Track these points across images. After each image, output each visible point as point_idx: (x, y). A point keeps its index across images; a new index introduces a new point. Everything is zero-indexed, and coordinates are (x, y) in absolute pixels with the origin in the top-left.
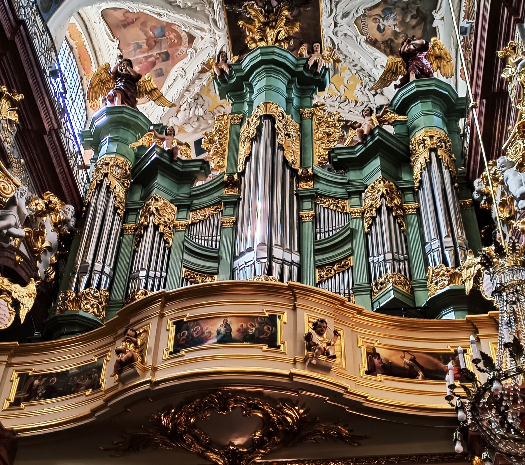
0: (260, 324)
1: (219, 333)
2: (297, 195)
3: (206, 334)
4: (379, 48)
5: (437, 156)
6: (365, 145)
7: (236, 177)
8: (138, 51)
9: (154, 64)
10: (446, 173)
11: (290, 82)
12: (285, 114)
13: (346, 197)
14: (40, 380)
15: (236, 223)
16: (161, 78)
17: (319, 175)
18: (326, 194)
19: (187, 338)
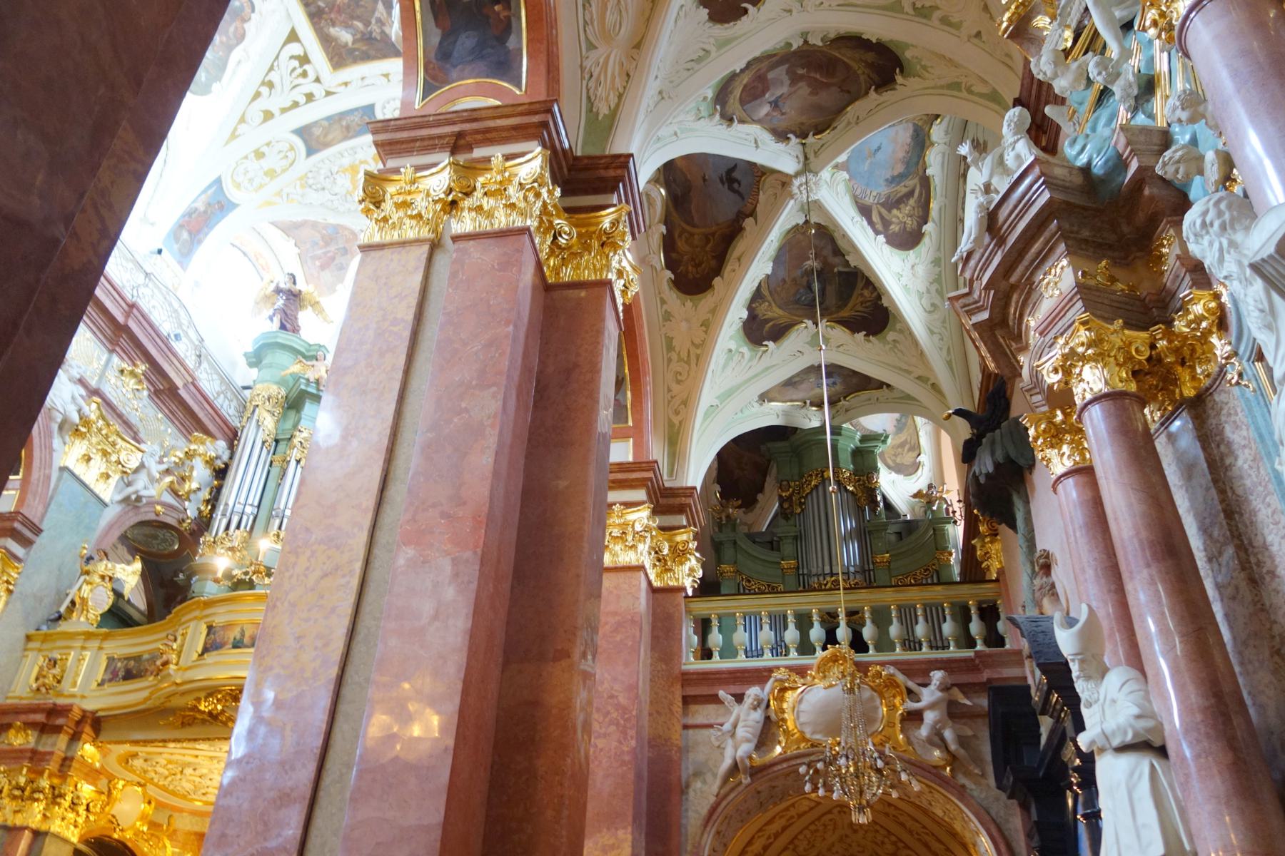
9: (333, 259)
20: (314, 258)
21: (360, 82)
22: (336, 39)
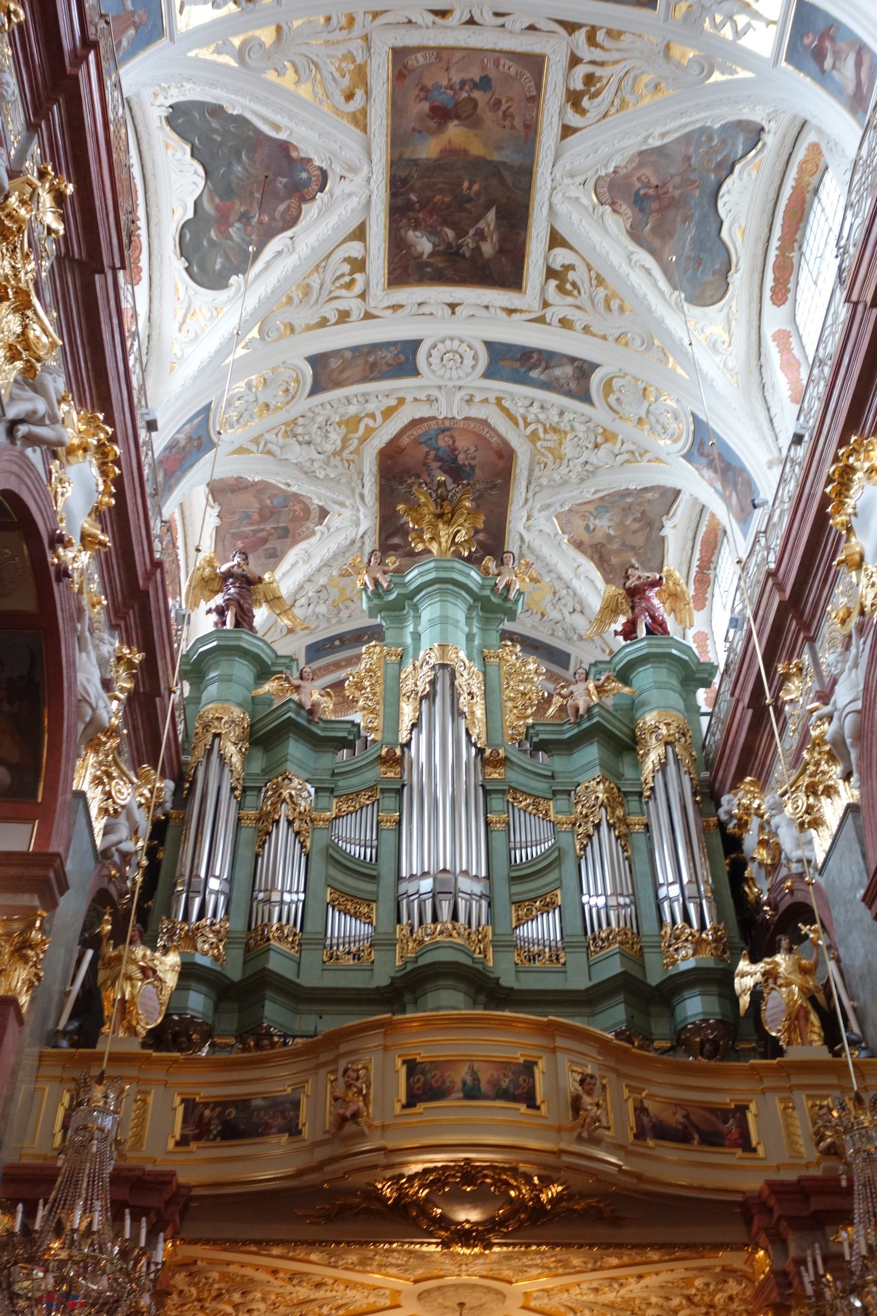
0: (514, 1073)
1: (464, 1083)
2: (483, 786)
3: (448, 1084)
4: (584, 552)
5: (675, 755)
6: (578, 724)
7: (398, 751)
8: (245, 522)
9: (265, 541)
10: (686, 779)
11: (470, 608)
12: (467, 662)
13: (550, 796)
14: (213, 1110)
15: (399, 823)
16: (272, 560)
17: (513, 759)
18: (523, 789)
19: (425, 1086)
20: (236, 536)
21: (415, 310)
22: (410, 246)
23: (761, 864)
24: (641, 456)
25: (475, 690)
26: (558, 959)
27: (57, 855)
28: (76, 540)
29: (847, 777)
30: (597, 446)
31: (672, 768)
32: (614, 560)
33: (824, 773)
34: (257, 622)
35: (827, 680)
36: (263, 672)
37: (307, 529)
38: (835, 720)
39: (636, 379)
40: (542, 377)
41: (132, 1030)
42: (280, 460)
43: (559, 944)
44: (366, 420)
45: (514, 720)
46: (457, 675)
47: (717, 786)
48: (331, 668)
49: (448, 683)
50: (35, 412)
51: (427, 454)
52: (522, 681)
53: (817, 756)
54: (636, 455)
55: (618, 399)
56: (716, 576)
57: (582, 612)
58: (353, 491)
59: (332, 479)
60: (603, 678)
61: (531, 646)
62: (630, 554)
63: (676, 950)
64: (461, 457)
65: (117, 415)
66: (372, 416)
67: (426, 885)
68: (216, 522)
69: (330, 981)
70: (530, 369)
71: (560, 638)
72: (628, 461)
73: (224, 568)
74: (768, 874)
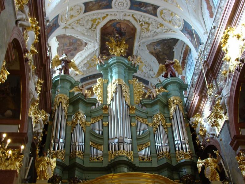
2: (129, 115)
5: (178, 108)
6: (154, 100)
8: (65, 46)
9: (70, 51)
13: (147, 118)
15: (108, 125)
16: (72, 56)
17: (137, 108)
18: (140, 116)
23: (201, 135)
24: (170, 30)
25: (127, 91)
26: (150, 159)
27: (26, 133)
28: (30, 51)
29: (225, 113)
30: (158, 28)
31: (178, 111)
32: (161, 57)
33: (219, 112)
34: (70, 72)
35: (220, 89)
36: (72, 86)
37: (82, 48)
38: (222, 99)
39: (169, 11)
40: (144, 9)
41: (45, 179)
42: (76, 30)
43: (150, 155)
44: (98, 20)
45: (138, 98)
46: (122, 86)
47: (189, 115)
48: (87, 84)
49: (120, 88)
50: (23, 18)
51: (114, 29)
52: (138, 88)
53: (217, 108)
54: (169, 30)
55: (164, 16)
56: (187, 61)
57: (152, 70)
58: (94, 38)
59: (89, 35)
60: (160, 88)
61: (140, 79)
62: (165, 56)
63: (180, 157)
64: (122, 30)
65: (40, 19)
66: (100, 19)
67: (116, 141)
68: (57, 46)
69: (91, 165)
70: (141, 7)
71: (146, 77)
72: (166, 32)
73: (61, 58)
74: (202, 138)
